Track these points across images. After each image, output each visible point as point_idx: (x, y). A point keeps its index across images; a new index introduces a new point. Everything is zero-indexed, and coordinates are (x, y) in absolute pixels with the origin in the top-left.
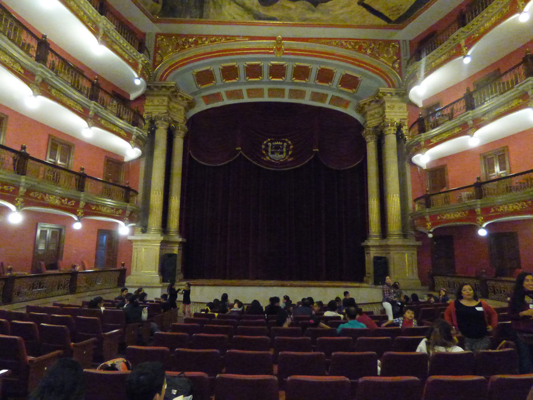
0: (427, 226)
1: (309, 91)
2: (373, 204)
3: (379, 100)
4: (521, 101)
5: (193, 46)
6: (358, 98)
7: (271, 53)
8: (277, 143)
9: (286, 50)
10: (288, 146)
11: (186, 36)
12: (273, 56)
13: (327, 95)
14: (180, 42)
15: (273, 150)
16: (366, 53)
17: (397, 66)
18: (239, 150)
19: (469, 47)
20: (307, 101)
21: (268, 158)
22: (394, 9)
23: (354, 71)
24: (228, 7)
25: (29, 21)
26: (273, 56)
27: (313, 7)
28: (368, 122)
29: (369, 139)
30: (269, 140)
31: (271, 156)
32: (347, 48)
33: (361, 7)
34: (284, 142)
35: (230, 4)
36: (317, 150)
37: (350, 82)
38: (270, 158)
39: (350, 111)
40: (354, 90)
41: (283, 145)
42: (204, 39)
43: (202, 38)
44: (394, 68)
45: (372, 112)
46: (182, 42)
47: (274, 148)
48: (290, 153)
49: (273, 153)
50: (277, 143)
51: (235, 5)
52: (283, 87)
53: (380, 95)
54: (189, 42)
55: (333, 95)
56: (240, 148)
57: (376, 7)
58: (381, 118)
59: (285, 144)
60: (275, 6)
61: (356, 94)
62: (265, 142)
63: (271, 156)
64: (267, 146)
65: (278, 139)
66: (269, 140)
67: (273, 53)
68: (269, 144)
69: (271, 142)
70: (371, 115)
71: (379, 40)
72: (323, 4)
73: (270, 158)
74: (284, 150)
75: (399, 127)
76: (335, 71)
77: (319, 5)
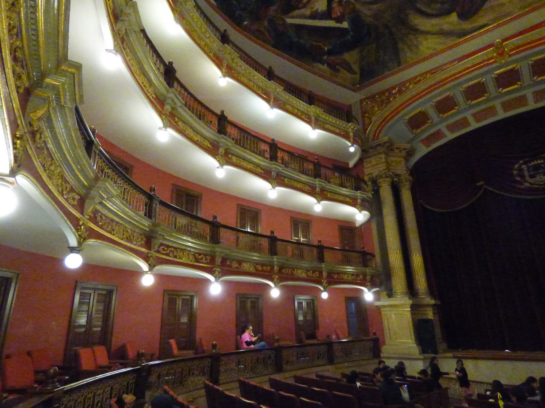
5: (397, 95)
7: (491, 64)
8: (536, 162)
9: (511, 51)
11: (387, 90)
12: (495, 65)
14: (384, 98)
15: (532, 173)
18: (482, 185)
21: (527, 184)
24: (424, 42)
25: (242, 124)
26: (495, 65)
30: (521, 162)
31: (532, 181)
38: (531, 184)
43: (405, 85)
47: (532, 170)
49: (532, 177)
50: (536, 162)
54: (393, 94)
56: (482, 183)
60: (481, 13)
63: (532, 181)
64: (520, 170)
65: (535, 157)
66: (521, 162)
68: (524, 166)
69: (525, 163)
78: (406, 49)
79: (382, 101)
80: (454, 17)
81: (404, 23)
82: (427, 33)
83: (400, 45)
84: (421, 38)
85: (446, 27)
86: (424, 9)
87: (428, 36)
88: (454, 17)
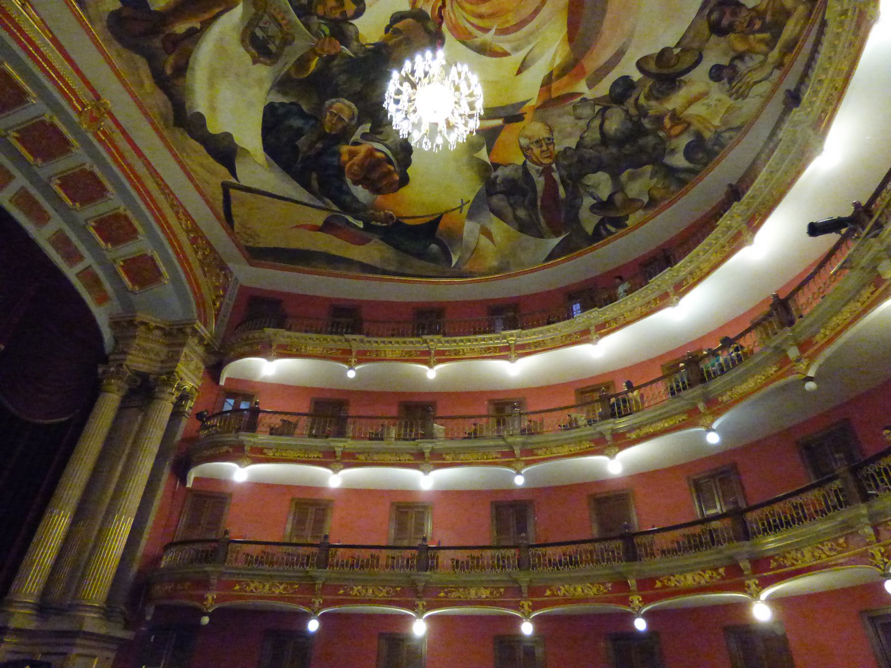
0: (207, 599)
1: (56, 223)
2: (59, 523)
3: (175, 334)
4: (412, 458)
6: (128, 306)
7: (75, 108)
9: (104, 133)
12: (75, 116)
13: (81, 258)
16: (196, 253)
17: (218, 304)
19: (359, 362)
22: (249, 232)
23: (167, 262)
26: (75, 116)
27: (171, 122)
28: (129, 357)
29: (114, 388)
32: (181, 224)
33: (221, 191)
37: (143, 271)
39: (101, 315)
40: (137, 288)
44: (214, 304)
45: (148, 345)
52: (14, 171)
53: (188, 330)
55: (90, 266)
57: (234, 210)
58: (159, 365)
60: (126, 53)
61: (132, 297)
67: (80, 113)
70: (145, 351)
71: (217, 253)
72: (186, 134)
75: (184, 397)
76: (140, 237)
77: (182, 129)
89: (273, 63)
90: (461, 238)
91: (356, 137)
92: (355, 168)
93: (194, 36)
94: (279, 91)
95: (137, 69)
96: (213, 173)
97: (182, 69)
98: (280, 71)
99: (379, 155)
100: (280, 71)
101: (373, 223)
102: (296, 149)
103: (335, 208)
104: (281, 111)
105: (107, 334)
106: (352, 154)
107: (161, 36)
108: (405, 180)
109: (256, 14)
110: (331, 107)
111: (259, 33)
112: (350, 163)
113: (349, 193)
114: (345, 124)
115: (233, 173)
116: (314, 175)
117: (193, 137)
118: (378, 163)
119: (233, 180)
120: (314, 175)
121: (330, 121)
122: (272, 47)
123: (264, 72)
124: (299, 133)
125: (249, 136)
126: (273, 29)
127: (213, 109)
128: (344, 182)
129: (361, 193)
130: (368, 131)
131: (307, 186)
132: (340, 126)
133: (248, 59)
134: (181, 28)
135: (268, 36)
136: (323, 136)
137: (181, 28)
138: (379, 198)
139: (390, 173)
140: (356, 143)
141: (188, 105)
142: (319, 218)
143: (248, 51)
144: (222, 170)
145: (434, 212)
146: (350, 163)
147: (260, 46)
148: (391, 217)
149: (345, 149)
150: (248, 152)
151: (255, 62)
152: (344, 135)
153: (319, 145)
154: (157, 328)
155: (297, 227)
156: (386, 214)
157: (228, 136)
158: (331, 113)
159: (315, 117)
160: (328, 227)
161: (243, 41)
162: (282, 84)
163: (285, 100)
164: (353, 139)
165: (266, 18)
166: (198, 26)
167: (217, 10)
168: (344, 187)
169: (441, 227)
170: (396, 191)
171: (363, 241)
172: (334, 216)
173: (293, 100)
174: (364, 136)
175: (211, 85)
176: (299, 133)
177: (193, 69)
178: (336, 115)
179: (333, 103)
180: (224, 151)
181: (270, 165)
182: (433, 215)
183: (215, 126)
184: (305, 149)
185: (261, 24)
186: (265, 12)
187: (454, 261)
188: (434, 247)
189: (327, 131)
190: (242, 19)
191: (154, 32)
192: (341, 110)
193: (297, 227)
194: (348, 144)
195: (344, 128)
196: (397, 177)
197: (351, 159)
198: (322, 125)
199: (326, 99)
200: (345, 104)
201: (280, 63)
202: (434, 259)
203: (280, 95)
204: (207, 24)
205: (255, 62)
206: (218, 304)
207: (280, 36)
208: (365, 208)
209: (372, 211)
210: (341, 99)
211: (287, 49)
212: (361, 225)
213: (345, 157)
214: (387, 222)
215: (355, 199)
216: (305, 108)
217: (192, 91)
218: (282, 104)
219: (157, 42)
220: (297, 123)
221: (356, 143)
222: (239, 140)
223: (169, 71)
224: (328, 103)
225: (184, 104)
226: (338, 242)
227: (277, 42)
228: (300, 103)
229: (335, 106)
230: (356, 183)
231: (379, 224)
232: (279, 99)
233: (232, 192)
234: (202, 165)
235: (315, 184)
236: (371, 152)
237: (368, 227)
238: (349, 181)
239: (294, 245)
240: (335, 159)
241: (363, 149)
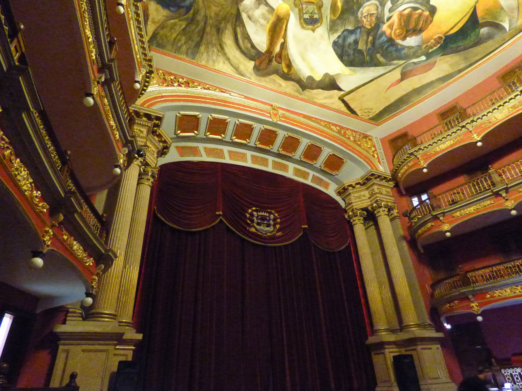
5: (183, 86)
8: (263, 214)
9: (282, 117)
10: (275, 220)
15: (259, 221)
17: (376, 155)
18: (220, 215)
20: (290, 174)
21: (253, 230)
22: (366, 111)
24: (221, 64)
27: (301, 90)
28: (353, 204)
30: (254, 209)
31: (258, 227)
33: (341, 102)
34: (270, 213)
35: (224, 63)
36: (307, 226)
38: (256, 229)
41: (269, 216)
42: (196, 84)
43: (194, 82)
46: (170, 79)
47: (260, 219)
48: (278, 226)
49: (258, 224)
50: (263, 214)
51: (229, 65)
54: (178, 82)
56: (221, 213)
57: (352, 106)
58: (369, 200)
59: (272, 216)
60: (267, 79)
62: (250, 211)
63: (258, 227)
64: (252, 215)
65: (263, 209)
66: (254, 209)
67: (270, 117)
68: (255, 213)
69: (256, 211)
73: (256, 229)
74: (272, 222)
77: (307, 90)
78: (205, 55)
79: (165, 79)
80: (252, 63)
81: (219, 31)
82: (228, 59)
83: (202, 48)
84: (221, 59)
85: (242, 68)
86: (239, 36)
87: (226, 62)
88: (252, 63)
89: (321, 24)
90: (502, 8)
91: (387, 14)
92: (398, 31)
93: (283, 46)
94: (333, 33)
95: (274, 80)
96: (331, 97)
97: (289, 66)
98: (327, 22)
99: (406, 12)
100: (327, 22)
101: (430, 51)
102: (361, 52)
103: (401, 62)
104: (340, 41)
105: (338, 199)
106: (391, 27)
107: (274, 59)
108: (433, 10)
109: (299, 10)
110: (362, 14)
111: (306, 16)
112: (393, 31)
113: (404, 47)
114: (376, 15)
115: (340, 89)
116: (378, 56)
117: (312, 89)
118: (410, 16)
119: (342, 93)
120: (378, 56)
121: (367, 21)
122: (316, 16)
123: (322, 30)
124: (356, 42)
125: (335, 66)
126: (311, 8)
127: (312, 69)
128: (398, 44)
129: (412, 41)
130: (391, 6)
131: (378, 64)
132: (374, 19)
133: (310, 32)
134: (277, 49)
135: (311, 13)
136: (368, 33)
137: (277, 49)
138: (424, 35)
139: (420, 15)
140: (389, 19)
141: (302, 77)
142: (397, 74)
143: (308, 29)
144: (335, 92)
145: (468, 10)
146: (393, 31)
147: (311, 22)
148: (440, 38)
149: (385, 27)
150: (339, 74)
151: (313, 31)
152: (379, 21)
153: (371, 38)
154: (357, 184)
155: (388, 89)
156: (435, 40)
157: (327, 75)
158: (365, 17)
159: (359, 27)
160: (404, 76)
161: (303, 27)
162: (332, 28)
163: (339, 34)
164: (386, 18)
165: (304, 6)
166: (282, 40)
167: (284, 26)
168: (399, 47)
169: (479, 13)
170: (431, 21)
171: (430, 67)
172: (403, 68)
173: (342, 30)
174: (391, 11)
175: (304, 59)
176: (356, 42)
177: (293, 60)
178: (368, 15)
179: (362, 11)
180: (330, 84)
181: (354, 71)
182: (469, 12)
183: (318, 77)
184: (365, 47)
185: (304, 12)
186: (302, 4)
187: (506, 25)
188: (484, 30)
189: (369, 27)
190: (296, 19)
191: (270, 61)
192: (368, 10)
193: (388, 89)
194: (385, 23)
195: (377, 18)
196: (427, 13)
197: (392, 30)
198: (365, 28)
199: (357, 13)
200: (368, 5)
201: (324, 20)
202: (490, 37)
203: (335, 34)
204: (285, 37)
205: (313, 31)
206: (376, 155)
207: (315, 7)
208: (419, 46)
209: (424, 46)
210: (364, 5)
211: (323, 9)
212: (423, 58)
213: (388, 32)
214: (439, 43)
215: (410, 48)
216: (350, 28)
217: (300, 70)
218: (339, 37)
219: (274, 63)
220: (351, 39)
221: (389, 19)
222: (332, 73)
223: (286, 71)
224: (359, 14)
225: (300, 79)
226: (416, 78)
227: (316, 11)
228: (346, 28)
229: (364, 12)
230: (404, 39)
231: (435, 48)
232: (334, 37)
233: (345, 98)
234: (326, 98)
235: (382, 59)
236: (401, 15)
237: (429, 56)
238: (399, 41)
239: (392, 100)
240: (384, 38)
241: (395, 18)
